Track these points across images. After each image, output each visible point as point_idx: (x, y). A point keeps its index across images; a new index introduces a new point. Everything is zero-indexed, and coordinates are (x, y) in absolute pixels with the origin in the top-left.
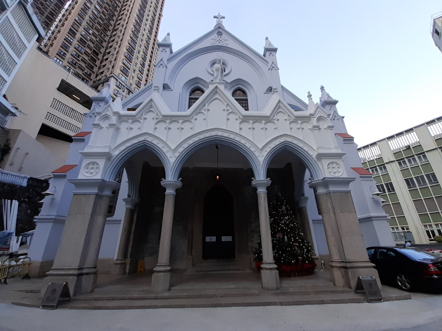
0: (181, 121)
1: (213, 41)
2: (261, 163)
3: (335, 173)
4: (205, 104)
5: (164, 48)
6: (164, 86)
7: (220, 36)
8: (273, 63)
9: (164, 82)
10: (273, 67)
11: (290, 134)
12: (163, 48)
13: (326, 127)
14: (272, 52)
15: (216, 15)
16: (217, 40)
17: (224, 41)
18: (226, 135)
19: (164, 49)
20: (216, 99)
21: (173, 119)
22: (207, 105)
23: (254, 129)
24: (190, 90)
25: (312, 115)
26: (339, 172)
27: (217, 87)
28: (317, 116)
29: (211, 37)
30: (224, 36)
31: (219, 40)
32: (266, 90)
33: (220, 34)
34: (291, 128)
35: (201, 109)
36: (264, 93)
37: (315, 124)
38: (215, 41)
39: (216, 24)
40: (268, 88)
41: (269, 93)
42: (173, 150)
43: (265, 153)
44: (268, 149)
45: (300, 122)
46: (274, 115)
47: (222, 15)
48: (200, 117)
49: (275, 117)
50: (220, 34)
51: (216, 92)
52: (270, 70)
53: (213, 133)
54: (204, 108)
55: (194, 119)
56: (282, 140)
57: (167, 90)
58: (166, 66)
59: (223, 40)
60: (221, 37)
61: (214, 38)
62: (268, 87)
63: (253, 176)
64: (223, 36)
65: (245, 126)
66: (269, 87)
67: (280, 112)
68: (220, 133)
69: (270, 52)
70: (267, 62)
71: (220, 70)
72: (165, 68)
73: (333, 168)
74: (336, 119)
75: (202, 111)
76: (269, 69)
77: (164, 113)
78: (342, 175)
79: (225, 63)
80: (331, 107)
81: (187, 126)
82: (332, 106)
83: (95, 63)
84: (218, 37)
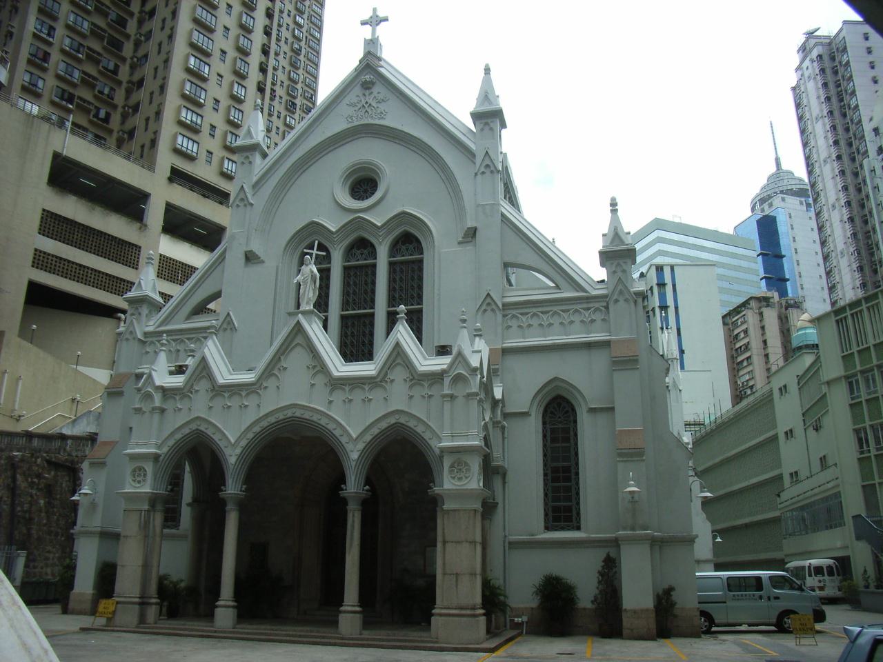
0: (244, 394)
1: (351, 111)
2: (353, 464)
3: (460, 479)
4: (280, 358)
5: (248, 154)
6: (246, 255)
7: (367, 92)
8: (487, 157)
9: (247, 244)
10: (487, 166)
11: (407, 410)
12: (245, 154)
13: (465, 394)
14: (489, 121)
15: (366, 17)
16: (359, 106)
17: (379, 105)
18: (307, 415)
19: (247, 157)
20: (298, 344)
21: (234, 390)
22: (282, 358)
23: (351, 401)
24: (298, 256)
25: (443, 372)
26: (466, 478)
27: (298, 322)
28: (453, 373)
29: (346, 101)
30: (378, 89)
31: (367, 103)
32: (463, 236)
33: (367, 86)
34: (411, 397)
35: (273, 369)
36: (460, 243)
37: (447, 391)
38: (357, 109)
39: (361, 55)
40: (466, 231)
41: (471, 241)
42: (233, 445)
43: (361, 446)
44: (368, 438)
45: (426, 385)
46: (386, 374)
47: (381, 14)
48: (271, 383)
49: (389, 376)
50: (367, 86)
51: (299, 330)
52: (479, 176)
53: (289, 413)
54: (279, 366)
55: (262, 387)
56: (392, 420)
57: (252, 263)
58: (252, 205)
59: (374, 104)
60: (372, 93)
61: (355, 100)
62: (466, 229)
63: (345, 483)
64: (376, 90)
65: (339, 396)
66: (468, 228)
67: (399, 364)
68: (298, 413)
69: (483, 121)
70: (474, 155)
71: (310, 279)
72: (249, 207)
73: (460, 469)
74: (621, 299)
75: (274, 372)
76: (476, 174)
77: (221, 381)
78: (466, 484)
79: (377, 170)
80: (617, 266)
81: (251, 401)
82: (621, 262)
83: (125, 28)
84: (364, 94)
